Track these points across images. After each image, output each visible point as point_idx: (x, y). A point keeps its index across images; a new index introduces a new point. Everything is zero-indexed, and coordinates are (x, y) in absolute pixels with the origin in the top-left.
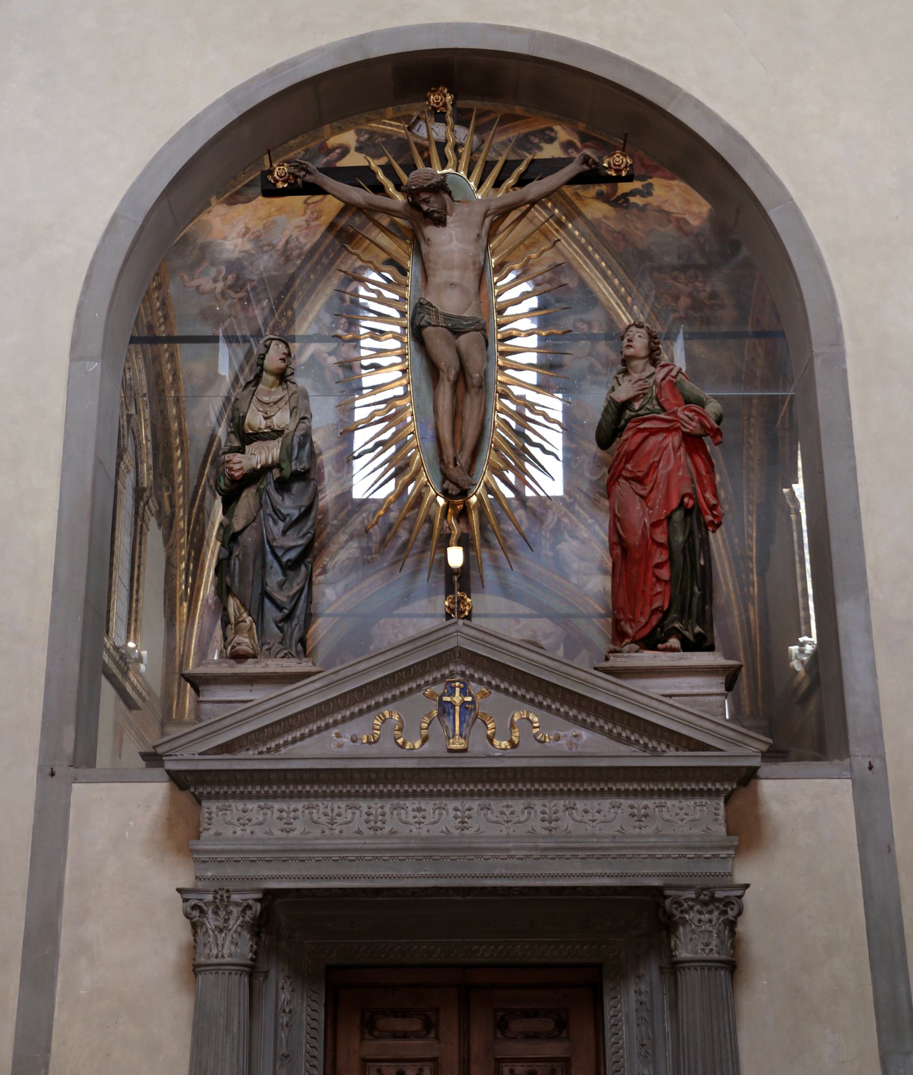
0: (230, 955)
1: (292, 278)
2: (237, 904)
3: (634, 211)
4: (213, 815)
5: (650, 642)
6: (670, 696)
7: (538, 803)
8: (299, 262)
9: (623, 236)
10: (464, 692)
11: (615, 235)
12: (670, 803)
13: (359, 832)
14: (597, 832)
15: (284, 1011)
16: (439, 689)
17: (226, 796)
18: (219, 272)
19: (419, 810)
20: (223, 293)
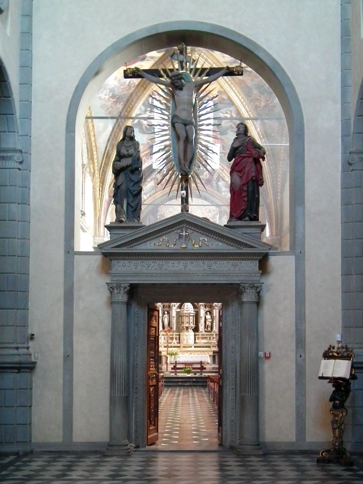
0: (121, 300)
2: (123, 287)
3: (248, 73)
4: (115, 264)
5: (240, 218)
6: (245, 233)
7: (206, 262)
8: (134, 89)
10: (186, 232)
11: (241, 81)
12: (243, 262)
13: (156, 269)
14: (222, 269)
15: (136, 313)
16: (179, 231)
17: (118, 259)
19: (173, 263)
20: (108, 99)
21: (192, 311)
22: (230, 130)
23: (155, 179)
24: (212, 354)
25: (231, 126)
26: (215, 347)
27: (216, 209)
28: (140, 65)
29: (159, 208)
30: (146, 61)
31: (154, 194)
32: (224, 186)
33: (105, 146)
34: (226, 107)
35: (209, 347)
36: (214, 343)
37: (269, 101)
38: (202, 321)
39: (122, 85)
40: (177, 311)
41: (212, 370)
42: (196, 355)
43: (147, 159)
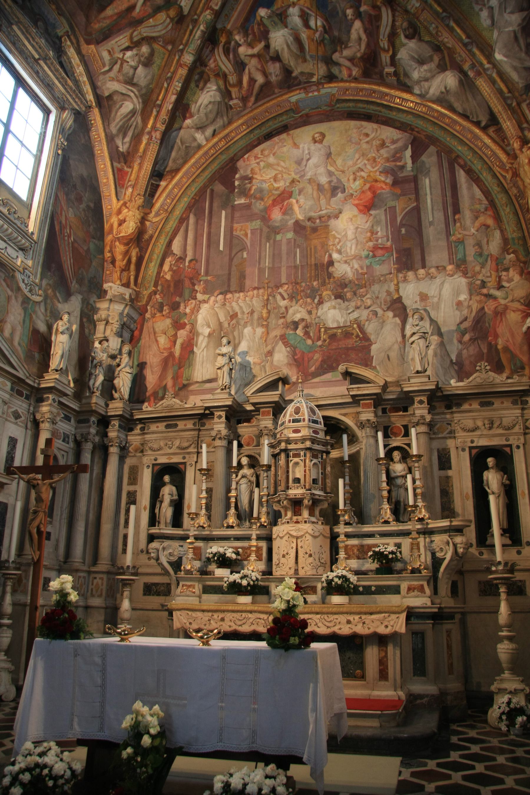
23: (217, 75)
27: (400, 136)
29: (240, 164)
31: (224, 127)
32: (413, 58)
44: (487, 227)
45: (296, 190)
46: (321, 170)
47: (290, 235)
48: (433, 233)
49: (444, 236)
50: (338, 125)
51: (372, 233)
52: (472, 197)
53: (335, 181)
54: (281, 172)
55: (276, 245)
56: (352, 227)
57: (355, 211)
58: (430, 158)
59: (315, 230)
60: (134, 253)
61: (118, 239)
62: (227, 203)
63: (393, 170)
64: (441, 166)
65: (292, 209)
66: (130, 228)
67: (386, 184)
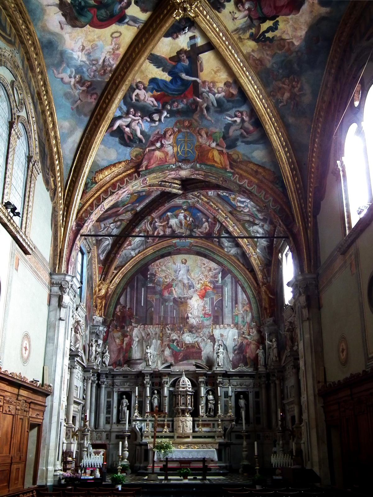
1: (108, 83)
3: (268, 42)
9: (261, 61)
11: (257, 62)
18: (72, 72)
20: (74, 85)
21: (189, 388)
22: (240, 140)
24: (217, 446)
25: (242, 134)
26: (221, 437)
28: (117, 32)
30: (126, 25)
33: (72, 156)
34: (236, 107)
35: (213, 437)
36: (220, 432)
37: (297, 87)
38: (203, 402)
39: (94, 65)
40: (170, 390)
41: (218, 471)
42: (196, 448)
43: (131, 180)
44: (247, 311)
45: (174, 284)
46: (185, 277)
47: (172, 304)
48: (227, 310)
49: (230, 312)
50: (193, 257)
51: (204, 308)
52: (243, 298)
53: (190, 283)
54: (168, 275)
55: (166, 307)
56: (196, 304)
57: (198, 298)
58: (228, 279)
59: (182, 303)
60: (104, 303)
61: (98, 297)
62: (144, 285)
63: (213, 282)
64: (232, 283)
65: (172, 292)
66: (103, 292)
67: (211, 288)
